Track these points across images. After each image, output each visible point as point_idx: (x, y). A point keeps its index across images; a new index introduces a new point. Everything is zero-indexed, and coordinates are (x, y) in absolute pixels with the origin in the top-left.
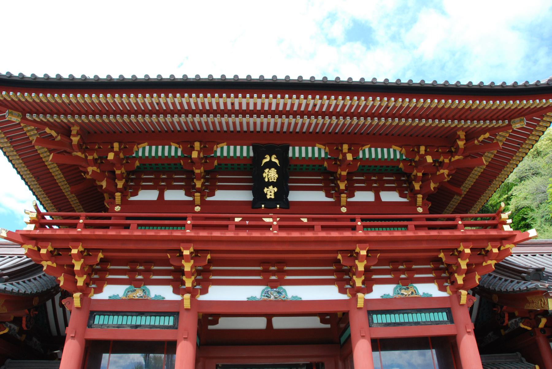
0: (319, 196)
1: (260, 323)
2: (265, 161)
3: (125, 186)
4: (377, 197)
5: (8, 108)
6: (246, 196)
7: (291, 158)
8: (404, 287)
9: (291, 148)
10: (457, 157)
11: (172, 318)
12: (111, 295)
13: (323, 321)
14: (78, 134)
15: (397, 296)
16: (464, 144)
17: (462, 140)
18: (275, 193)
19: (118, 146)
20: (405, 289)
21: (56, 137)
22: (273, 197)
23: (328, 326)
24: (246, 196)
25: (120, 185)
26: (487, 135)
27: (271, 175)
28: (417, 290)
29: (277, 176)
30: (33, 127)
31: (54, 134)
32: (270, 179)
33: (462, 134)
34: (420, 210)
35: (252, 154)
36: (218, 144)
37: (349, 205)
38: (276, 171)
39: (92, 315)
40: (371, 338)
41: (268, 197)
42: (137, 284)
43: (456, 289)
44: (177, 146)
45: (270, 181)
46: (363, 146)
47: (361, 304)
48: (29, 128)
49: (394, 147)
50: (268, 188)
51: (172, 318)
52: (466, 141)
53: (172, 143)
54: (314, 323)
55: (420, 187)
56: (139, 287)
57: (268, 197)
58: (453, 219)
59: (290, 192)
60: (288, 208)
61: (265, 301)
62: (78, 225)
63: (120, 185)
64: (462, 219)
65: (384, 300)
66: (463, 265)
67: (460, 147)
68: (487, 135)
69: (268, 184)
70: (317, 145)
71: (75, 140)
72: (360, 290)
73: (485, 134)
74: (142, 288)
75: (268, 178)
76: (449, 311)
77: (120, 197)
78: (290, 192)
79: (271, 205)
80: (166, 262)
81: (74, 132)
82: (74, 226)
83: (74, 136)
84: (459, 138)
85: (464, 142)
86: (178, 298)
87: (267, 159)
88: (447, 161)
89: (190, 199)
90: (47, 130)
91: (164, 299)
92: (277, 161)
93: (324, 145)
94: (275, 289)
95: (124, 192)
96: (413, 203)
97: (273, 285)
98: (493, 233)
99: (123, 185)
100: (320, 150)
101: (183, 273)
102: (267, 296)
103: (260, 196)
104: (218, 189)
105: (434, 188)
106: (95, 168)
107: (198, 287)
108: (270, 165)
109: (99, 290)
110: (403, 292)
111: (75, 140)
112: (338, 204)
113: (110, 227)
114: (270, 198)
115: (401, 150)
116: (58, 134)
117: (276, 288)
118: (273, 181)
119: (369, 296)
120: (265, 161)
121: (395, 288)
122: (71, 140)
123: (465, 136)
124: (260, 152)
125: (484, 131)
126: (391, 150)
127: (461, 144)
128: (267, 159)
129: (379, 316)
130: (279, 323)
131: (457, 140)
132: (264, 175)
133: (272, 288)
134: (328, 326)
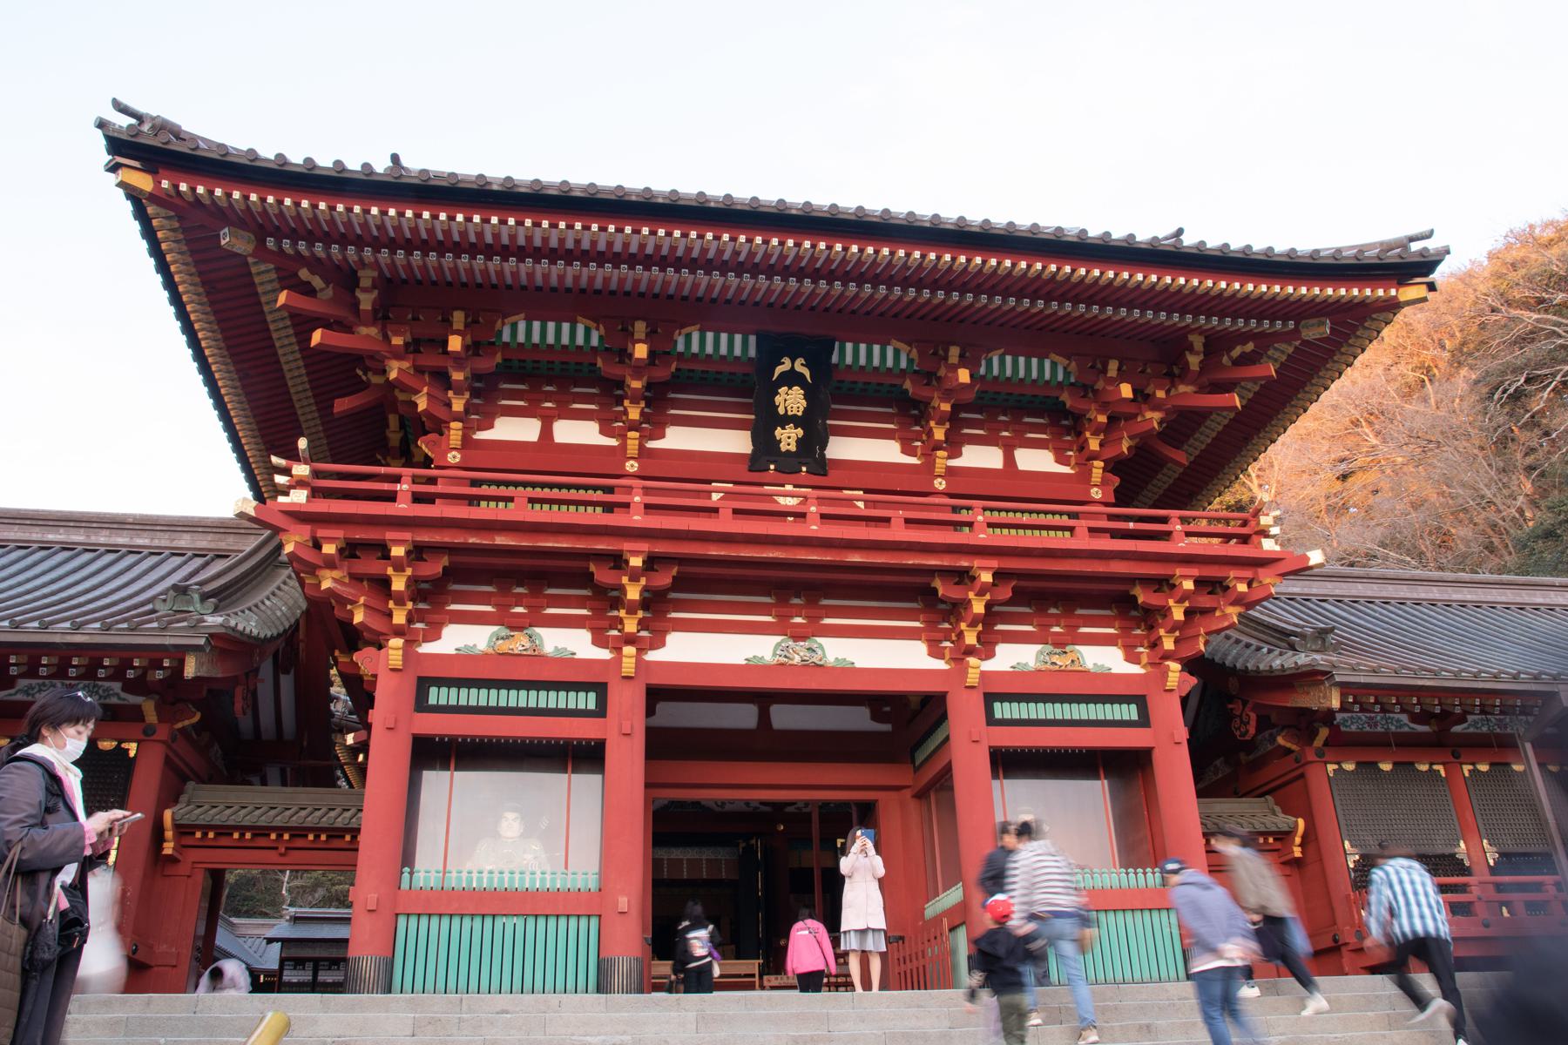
0: (887, 451)
1: (743, 717)
3: (468, 409)
4: (1009, 460)
5: (230, 223)
6: (738, 442)
7: (837, 365)
8: (1058, 651)
9: (837, 344)
10: (1182, 388)
11: (592, 696)
12: (460, 645)
13: (876, 717)
14: (374, 287)
15: (1043, 667)
16: (1201, 362)
17: (1197, 353)
18: (798, 441)
19: (463, 319)
20: (1059, 654)
21: (322, 290)
22: (793, 448)
23: (887, 727)
24: (738, 442)
25: (458, 405)
26: (1250, 346)
27: (792, 400)
28: (1082, 657)
29: (804, 403)
30: (272, 266)
31: (317, 282)
32: (789, 408)
33: (1198, 341)
34: (1096, 494)
35: (752, 353)
36: (683, 326)
37: (951, 472)
38: (802, 392)
39: (424, 684)
40: (990, 747)
41: (783, 447)
42: (517, 625)
44: (592, 324)
45: (790, 413)
46: (990, 350)
47: (973, 678)
48: (263, 267)
49: (1053, 356)
50: (783, 428)
51: (592, 696)
52: (1205, 355)
53: (579, 318)
54: (857, 719)
56: (520, 628)
57: (783, 447)
58: (1164, 520)
59: (832, 439)
60: (825, 475)
62: (399, 496)
63: (458, 405)
64: (1184, 520)
65: (1016, 675)
67: (1192, 368)
68: (1250, 346)
69: (785, 420)
70: (894, 341)
71: (366, 301)
72: (970, 651)
73: (1244, 343)
74: (529, 631)
75: (786, 408)
76: (1140, 701)
77: (460, 433)
78: (832, 439)
79: (789, 465)
80: (586, 579)
81: (365, 282)
82: (391, 497)
83: (365, 290)
84: (1191, 348)
85: (1201, 357)
87: (786, 365)
88: (1161, 394)
89: (613, 442)
90: (304, 274)
91: (576, 657)
92: (807, 373)
93: (910, 344)
94: (802, 643)
96: (1084, 476)
99: (465, 405)
100: (897, 352)
101: (617, 603)
102: (785, 657)
104: (672, 425)
105: (1128, 449)
106: (405, 365)
107: (644, 634)
108: (791, 379)
109: (434, 635)
110: (1055, 659)
111: (366, 301)
112: (928, 468)
113: (437, 500)
115: (1068, 365)
116: (327, 283)
118: (795, 415)
119: (989, 666)
120: (779, 370)
121: (1041, 652)
122: (356, 303)
123: (1205, 345)
124: (772, 349)
125: (1243, 337)
126: (1047, 364)
127: (1194, 361)
128: (786, 365)
129: (1006, 705)
130: (785, 717)
131: (1187, 353)
132: (778, 399)
133: (797, 638)
134: (887, 727)
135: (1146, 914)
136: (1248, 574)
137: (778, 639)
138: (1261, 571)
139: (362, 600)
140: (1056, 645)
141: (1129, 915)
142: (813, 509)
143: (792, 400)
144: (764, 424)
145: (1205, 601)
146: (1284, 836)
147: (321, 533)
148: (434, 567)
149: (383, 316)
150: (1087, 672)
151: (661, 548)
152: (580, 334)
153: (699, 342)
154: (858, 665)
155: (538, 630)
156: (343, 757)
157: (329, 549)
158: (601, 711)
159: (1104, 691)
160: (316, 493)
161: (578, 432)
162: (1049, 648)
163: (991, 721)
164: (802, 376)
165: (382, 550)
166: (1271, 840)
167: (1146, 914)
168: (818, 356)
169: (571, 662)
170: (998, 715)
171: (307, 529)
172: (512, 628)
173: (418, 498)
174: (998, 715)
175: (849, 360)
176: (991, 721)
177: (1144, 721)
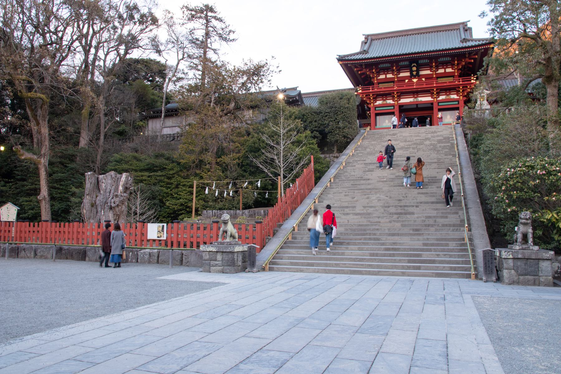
0: (428, 72)
1: (415, 106)
4: (445, 71)
25: (375, 75)
27: (414, 69)
39: (375, 108)
63: (375, 75)
69: (414, 71)
71: (364, 67)
76: (458, 101)
82: (370, 90)
86: (394, 102)
87: (413, 65)
88: (463, 60)
95: (377, 77)
97: (415, 98)
98: (469, 82)
103: (411, 74)
108: (414, 66)
109: (376, 102)
111: (364, 67)
127: (467, 56)
128: (413, 65)
130: (419, 106)
144: (411, 72)
145: (465, 89)
148: (375, 96)
149: (366, 68)
152: (388, 65)
153: (402, 63)
156: (367, 115)
158: (394, 108)
160: (362, 90)
161: (390, 76)
168: (417, 63)
169: (390, 104)
171: (362, 95)
173: (373, 89)
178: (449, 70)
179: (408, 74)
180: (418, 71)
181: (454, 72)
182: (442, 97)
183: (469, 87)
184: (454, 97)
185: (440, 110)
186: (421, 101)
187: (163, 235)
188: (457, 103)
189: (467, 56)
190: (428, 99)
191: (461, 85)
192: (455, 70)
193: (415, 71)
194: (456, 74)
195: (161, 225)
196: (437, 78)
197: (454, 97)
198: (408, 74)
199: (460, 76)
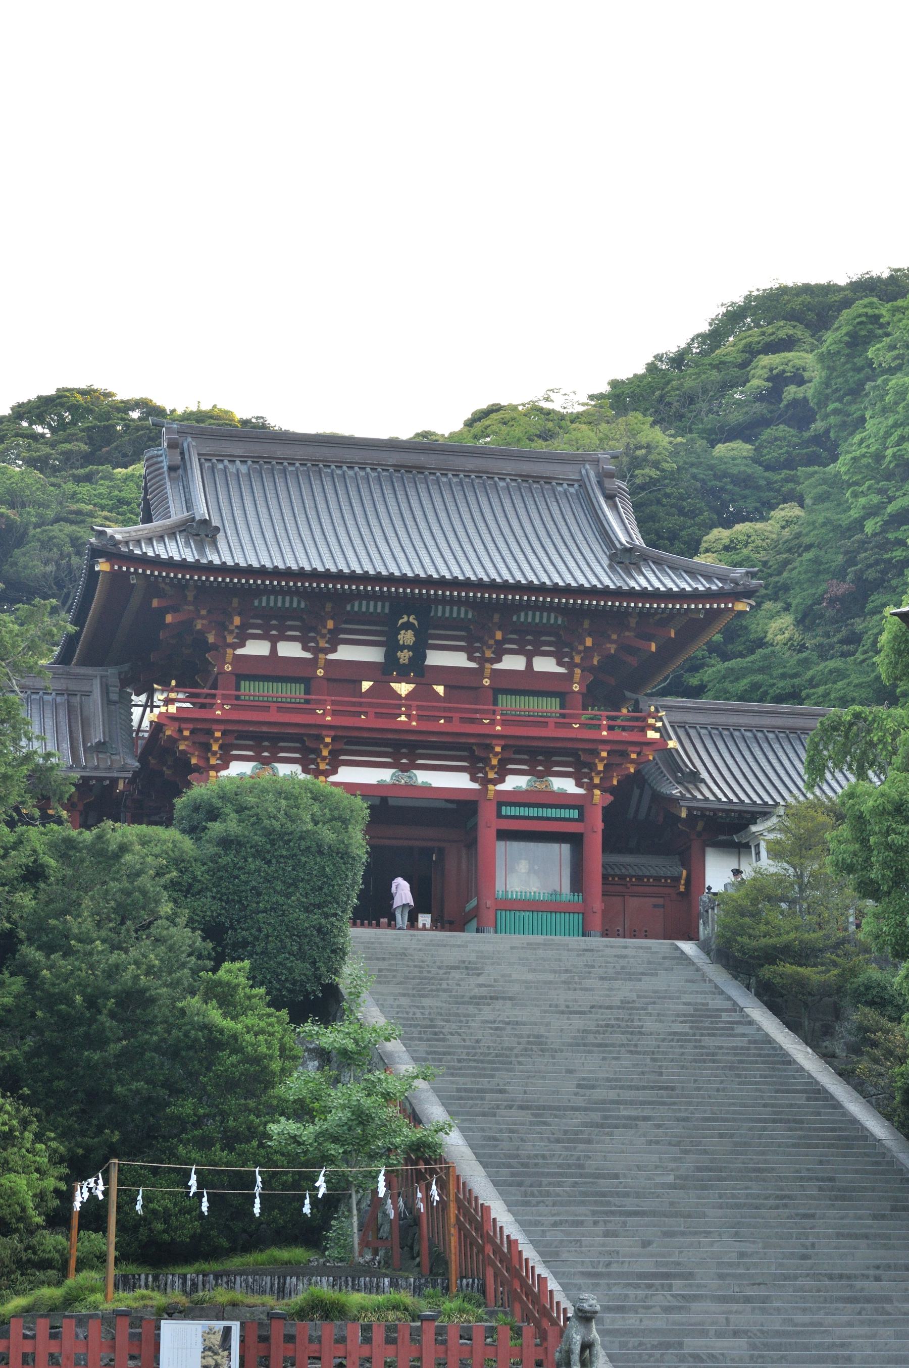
0: (458, 660)
2: (401, 621)
10: (627, 634)
18: (410, 659)
27: (407, 637)
31: (167, 588)
35: (387, 611)
43: (591, 787)
47: (491, 795)
55: (582, 659)
56: (267, 764)
61: (394, 785)
64: (609, 718)
65: (516, 792)
66: (600, 767)
69: (403, 647)
71: (190, 596)
76: (580, 808)
87: (405, 619)
88: (614, 637)
92: (416, 623)
97: (405, 769)
103: (391, 657)
105: (598, 662)
108: (407, 626)
114: (404, 664)
117: (406, 771)
119: (501, 787)
120: (401, 621)
121: (529, 781)
128: (405, 619)
129: (508, 808)
133: (403, 771)
135: (567, 915)
136: (638, 749)
137: (393, 771)
138: (645, 748)
139: (197, 753)
140: (538, 777)
141: (558, 915)
142: (414, 712)
143: (407, 637)
144: (392, 647)
145: (617, 760)
146: (677, 879)
147: (183, 726)
150: (553, 792)
151: (340, 733)
154: (434, 785)
155: (276, 765)
157: (186, 733)
159: (562, 801)
161: (290, 650)
162: (535, 779)
163: (499, 815)
164: (413, 624)
165: (210, 733)
166: (651, 880)
167: (567, 915)
170: (504, 813)
171: (176, 725)
172: (263, 764)
174: (504, 813)
175: (440, 614)
176: (499, 815)
177: (581, 819)
178: (545, 665)
179: (371, 655)
180: (419, 650)
181: (568, 678)
182: (514, 783)
183: (634, 756)
184: (566, 785)
185: (505, 835)
186: (429, 788)
187: (225, 1361)
188: (574, 814)
189: (633, 622)
190: (460, 781)
191: (604, 742)
192: (571, 666)
193: (409, 648)
194: (576, 688)
195: (219, 1325)
196: (497, 691)
197: (566, 785)
198: (371, 655)
199: (591, 697)
